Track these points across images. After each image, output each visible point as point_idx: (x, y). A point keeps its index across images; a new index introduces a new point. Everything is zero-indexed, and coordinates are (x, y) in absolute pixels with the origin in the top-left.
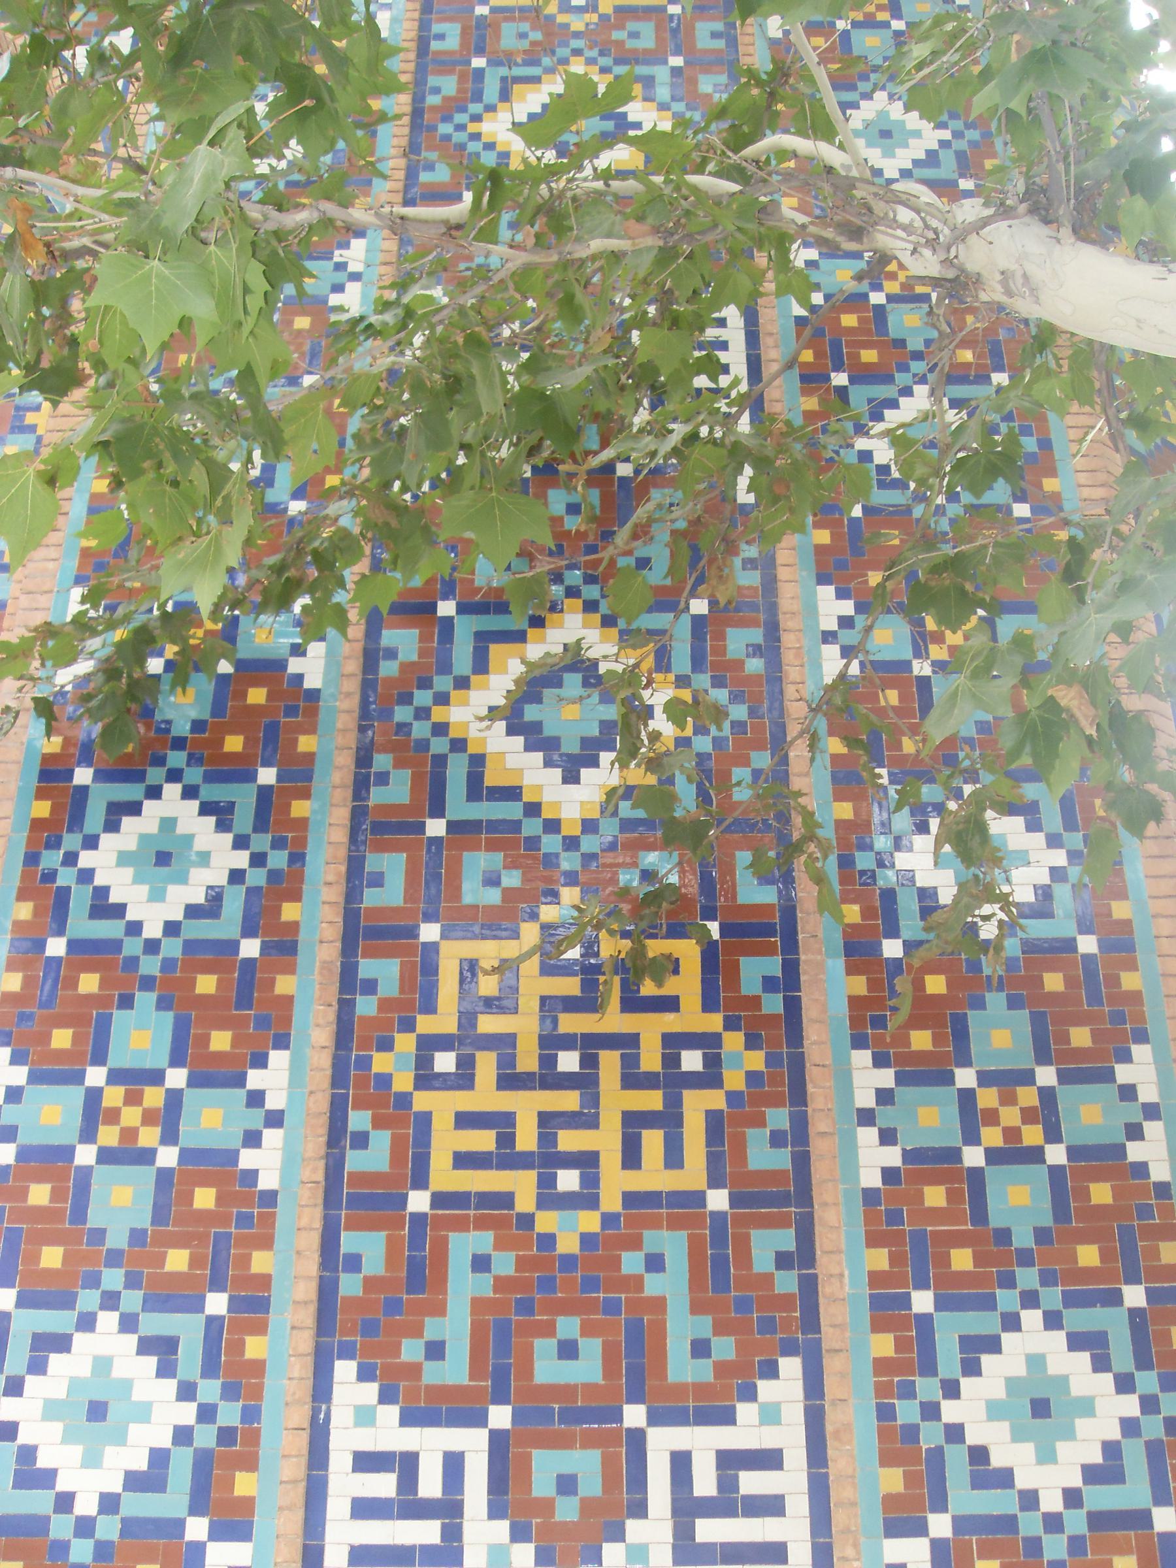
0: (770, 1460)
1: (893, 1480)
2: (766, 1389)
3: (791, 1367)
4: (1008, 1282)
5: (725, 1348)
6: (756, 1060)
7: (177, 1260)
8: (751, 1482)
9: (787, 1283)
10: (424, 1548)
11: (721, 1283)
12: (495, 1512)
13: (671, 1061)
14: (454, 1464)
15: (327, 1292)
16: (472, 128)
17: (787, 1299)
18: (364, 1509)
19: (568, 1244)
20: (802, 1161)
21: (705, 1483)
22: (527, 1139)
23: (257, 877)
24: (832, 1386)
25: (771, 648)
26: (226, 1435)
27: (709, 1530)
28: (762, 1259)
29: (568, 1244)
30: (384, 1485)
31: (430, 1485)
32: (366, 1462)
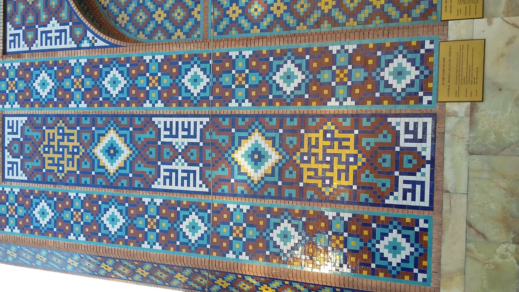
0: (407, 124)
1: (412, 102)
5: (385, 132)
6: (329, 123)
7: (366, 233)
8: (411, 128)
9: (373, 120)
10: (421, 188)
12: (415, 175)
14: (405, 182)
15: (371, 205)
16: (111, 175)
18: (413, 199)
19: (364, 160)
21: (411, 136)
22: (343, 167)
23: (290, 218)
25: (244, 116)
26: (399, 224)
27: (420, 136)
29: (364, 160)
30: (409, 195)
31: (409, 186)
32: (405, 198)
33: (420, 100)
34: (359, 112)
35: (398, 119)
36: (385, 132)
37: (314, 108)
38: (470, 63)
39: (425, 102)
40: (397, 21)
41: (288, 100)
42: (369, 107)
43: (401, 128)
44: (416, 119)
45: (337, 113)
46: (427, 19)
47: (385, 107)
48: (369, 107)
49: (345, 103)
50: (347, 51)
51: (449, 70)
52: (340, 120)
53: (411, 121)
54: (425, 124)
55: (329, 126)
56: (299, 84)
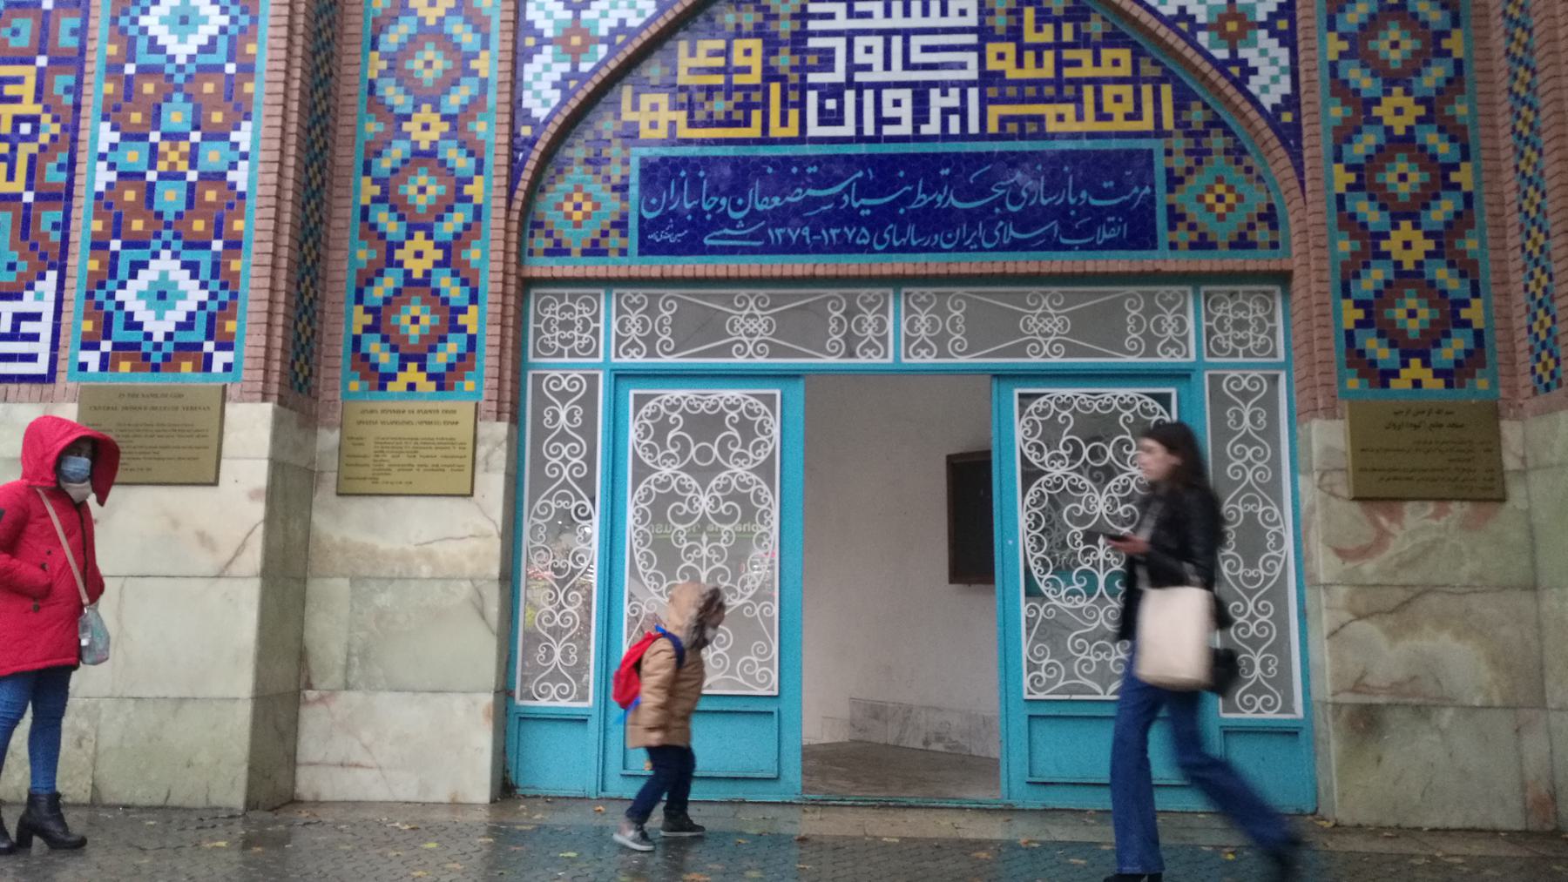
0: (36, 317)
1: (88, 326)
2: (39, 285)
3: (52, 276)
4: (158, 235)
8: (26, 327)
9: (56, 236)
11: (25, 235)
13: (16, 128)
17: (54, 245)
20: (70, 183)
24: (68, 283)
28: (45, 226)
33: (89, 345)
34: (76, 202)
35: (50, 296)
36: (23, 266)
37: (99, 89)
38: (164, 453)
39: (85, 356)
40: (359, 299)
41: (124, 21)
42: (86, 225)
43: (28, 303)
44: (46, 336)
45: (81, 146)
46: (353, 368)
47: (82, 263)
48: (86, 225)
49: (102, 165)
50: (233, 166)
51: (154, 408)
52: (63, 157)
53: (44, 328)
54: (32, 358)
55: (50, 128)
56: (162, 49)
